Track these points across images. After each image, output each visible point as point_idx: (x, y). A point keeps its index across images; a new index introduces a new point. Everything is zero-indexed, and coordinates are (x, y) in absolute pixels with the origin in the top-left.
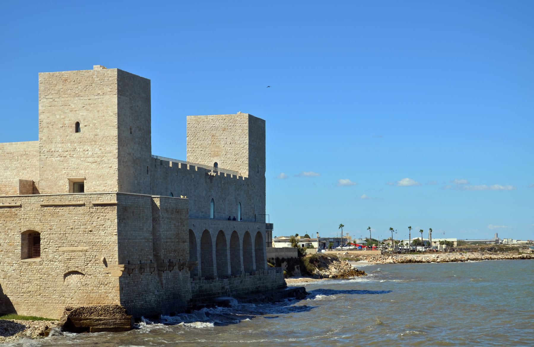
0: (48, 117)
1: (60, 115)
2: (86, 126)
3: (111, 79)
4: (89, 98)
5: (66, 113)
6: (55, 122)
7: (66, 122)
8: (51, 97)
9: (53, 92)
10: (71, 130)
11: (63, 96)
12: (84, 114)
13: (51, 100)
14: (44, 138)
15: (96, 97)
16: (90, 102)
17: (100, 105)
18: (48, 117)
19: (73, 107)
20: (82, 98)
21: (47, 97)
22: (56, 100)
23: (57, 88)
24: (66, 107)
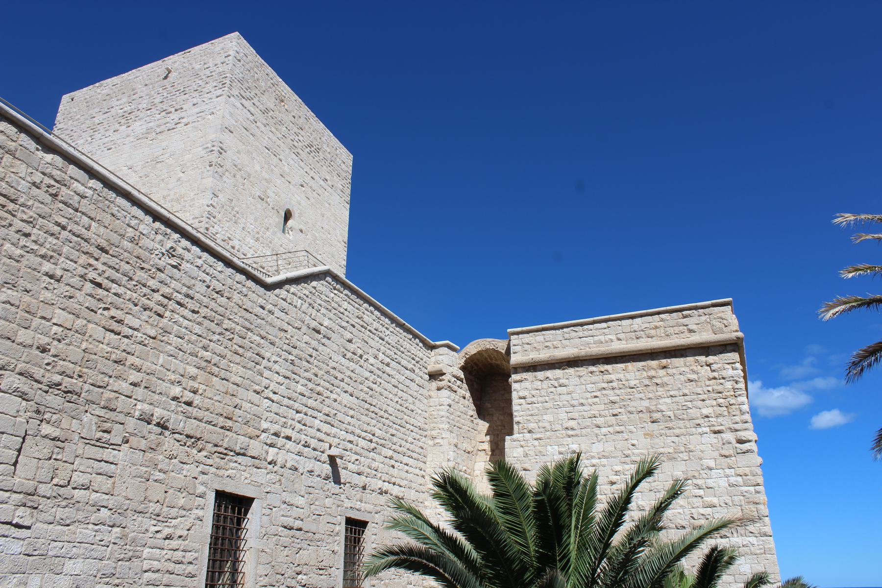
0: (239, 152)
1: (262, 168)
2: (301, 231)
3: (343, 166)
4: (312, 174)
5: (272, 170)
6: (249, 175)
7: (270, 193)
8: (252, 109)
9: (255, 101)
10: (277, 220)
11: (273, 129)
12: (303, 203)
13: (252, 118)
14: (221, 196)
15: (322, 183)
16: (312, 183)
17: (327, 205)
18: (239, 152)
19: (286, 168)
20: (302, 164)
21: (244, 101)
22: (258, 124)
23: (264, 98)
24: (275, 160)
